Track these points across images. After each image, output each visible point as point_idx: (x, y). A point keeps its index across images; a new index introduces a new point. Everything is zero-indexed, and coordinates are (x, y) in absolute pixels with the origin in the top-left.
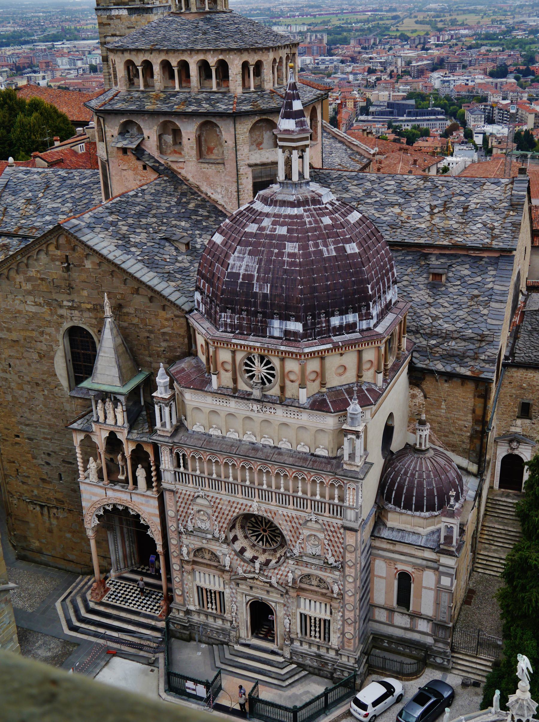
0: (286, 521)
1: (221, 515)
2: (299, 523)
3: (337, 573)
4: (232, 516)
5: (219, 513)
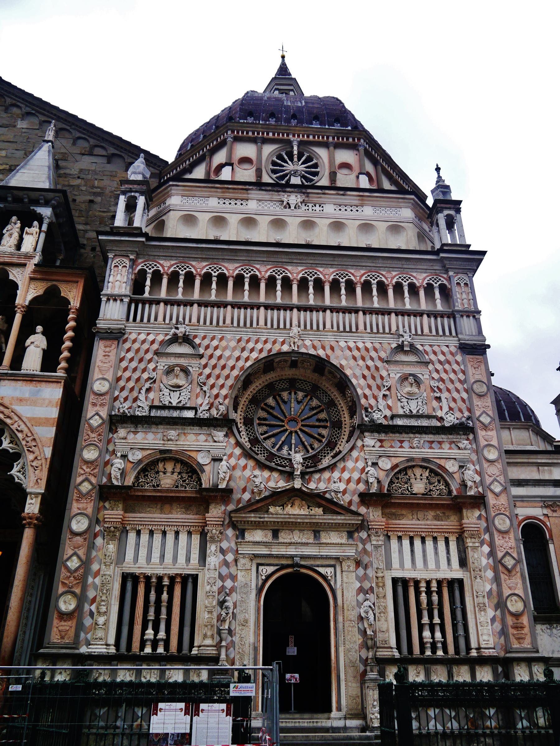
0: (355, 358)
1: (217, 371)
2: (380, 358)
4: (242, 368)
5: (214, 367)
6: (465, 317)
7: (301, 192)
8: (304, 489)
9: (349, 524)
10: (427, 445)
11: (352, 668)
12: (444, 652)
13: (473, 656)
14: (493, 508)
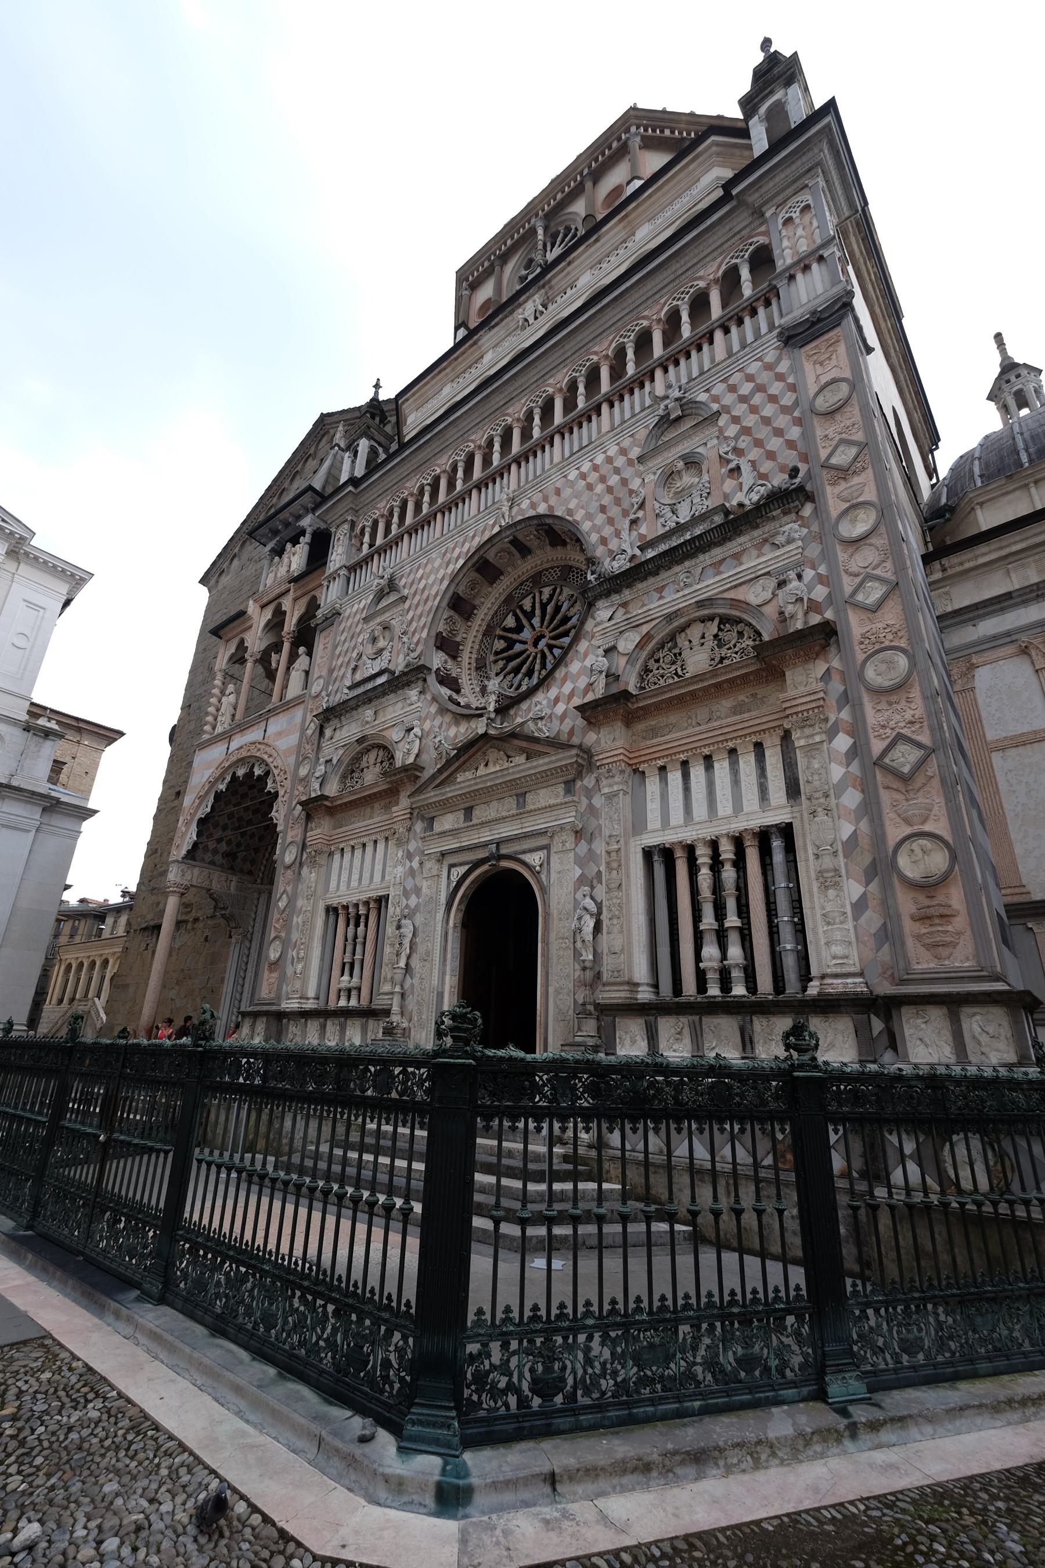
3: (791, 527)
6: (799, 277)
7: (540, 288)
8: (492, 732)
9: (560, 767)
10: (710, 571)
11: (562, 1024)
12: (748, 989)
14: (862, 643)
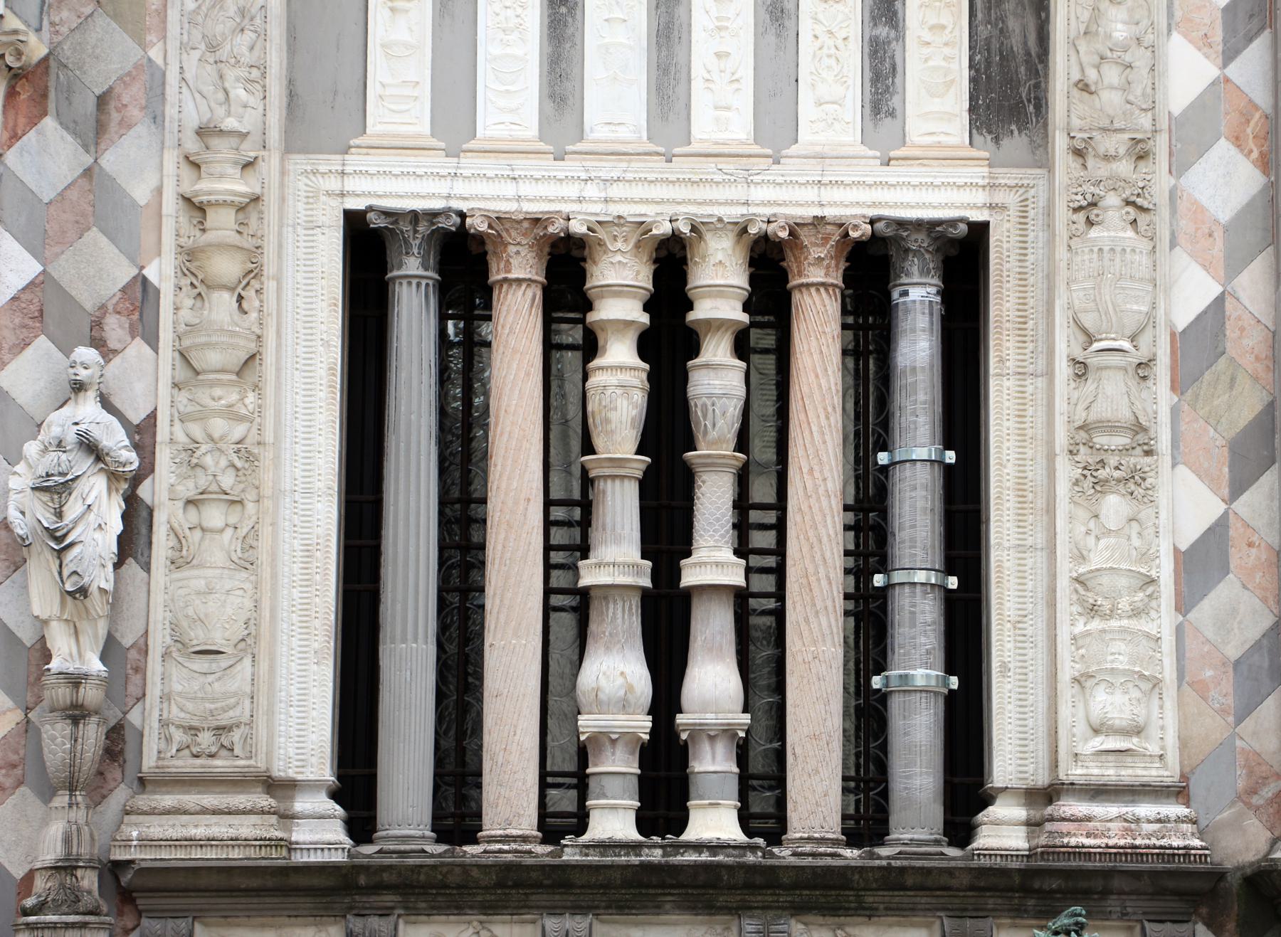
12: (745, 819)
13: (990, 853)
